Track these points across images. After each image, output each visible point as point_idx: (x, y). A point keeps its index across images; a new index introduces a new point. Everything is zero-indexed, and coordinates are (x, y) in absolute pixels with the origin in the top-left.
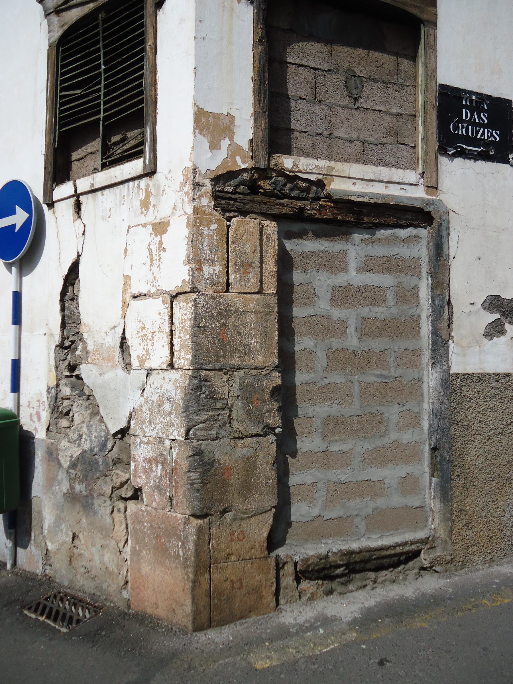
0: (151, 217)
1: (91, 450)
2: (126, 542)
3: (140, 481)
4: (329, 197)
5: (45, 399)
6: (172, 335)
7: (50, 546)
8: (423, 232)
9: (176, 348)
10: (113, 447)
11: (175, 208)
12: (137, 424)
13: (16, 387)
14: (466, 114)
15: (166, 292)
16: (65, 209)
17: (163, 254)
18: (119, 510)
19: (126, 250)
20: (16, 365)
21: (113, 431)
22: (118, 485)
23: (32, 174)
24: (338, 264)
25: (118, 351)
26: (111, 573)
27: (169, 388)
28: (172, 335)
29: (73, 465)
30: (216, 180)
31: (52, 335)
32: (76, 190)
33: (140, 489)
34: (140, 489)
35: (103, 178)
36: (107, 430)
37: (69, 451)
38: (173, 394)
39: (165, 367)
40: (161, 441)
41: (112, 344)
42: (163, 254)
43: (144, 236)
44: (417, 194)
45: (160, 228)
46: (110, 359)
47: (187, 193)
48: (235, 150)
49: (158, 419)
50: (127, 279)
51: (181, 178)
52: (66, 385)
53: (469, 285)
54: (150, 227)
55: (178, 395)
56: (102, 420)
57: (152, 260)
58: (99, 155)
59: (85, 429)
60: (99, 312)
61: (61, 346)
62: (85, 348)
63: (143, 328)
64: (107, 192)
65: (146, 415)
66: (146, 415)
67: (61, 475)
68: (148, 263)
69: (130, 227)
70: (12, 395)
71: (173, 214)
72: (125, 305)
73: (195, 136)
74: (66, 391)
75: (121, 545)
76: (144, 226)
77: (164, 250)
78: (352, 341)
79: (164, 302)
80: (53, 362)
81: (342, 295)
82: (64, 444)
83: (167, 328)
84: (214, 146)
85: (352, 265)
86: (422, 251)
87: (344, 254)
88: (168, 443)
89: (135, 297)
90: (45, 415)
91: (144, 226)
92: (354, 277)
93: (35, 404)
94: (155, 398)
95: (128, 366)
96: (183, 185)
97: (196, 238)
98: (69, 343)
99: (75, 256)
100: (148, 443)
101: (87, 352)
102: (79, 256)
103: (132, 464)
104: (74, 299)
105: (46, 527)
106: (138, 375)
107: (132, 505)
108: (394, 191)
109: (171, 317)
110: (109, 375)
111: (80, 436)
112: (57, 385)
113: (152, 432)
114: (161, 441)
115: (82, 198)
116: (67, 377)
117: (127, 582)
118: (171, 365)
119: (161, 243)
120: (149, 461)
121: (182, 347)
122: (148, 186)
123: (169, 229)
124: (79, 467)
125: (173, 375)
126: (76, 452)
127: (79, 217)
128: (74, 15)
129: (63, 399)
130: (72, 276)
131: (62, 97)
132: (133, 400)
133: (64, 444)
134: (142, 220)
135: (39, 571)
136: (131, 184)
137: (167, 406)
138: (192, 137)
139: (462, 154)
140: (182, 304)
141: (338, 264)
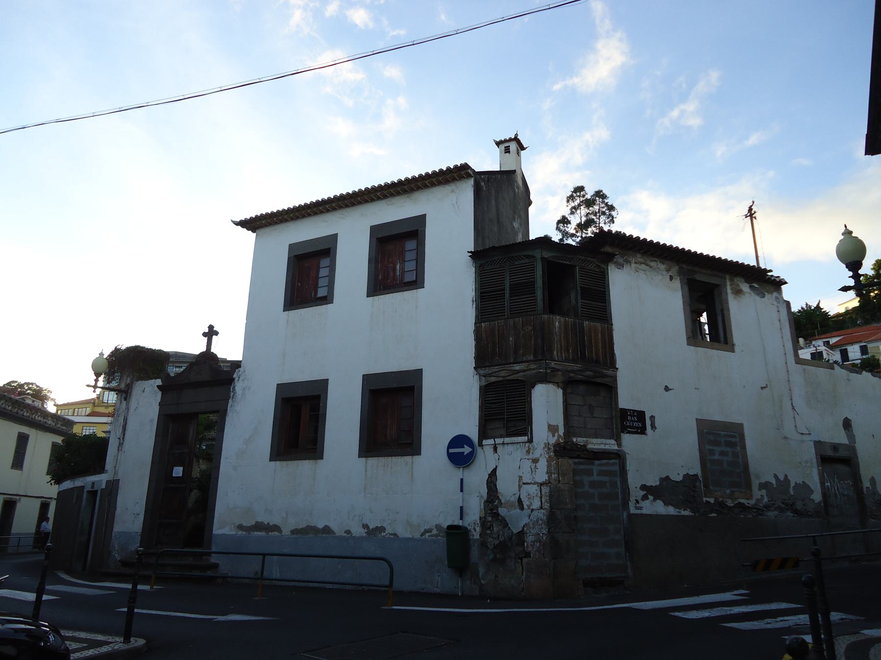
0: (531, 456)
4: (587, 450)
8: (617, 461)
13: (461, 518)
14: (629, 418)
16: (489, 450)
24: (590, 473)
27: (541, 515)
29: (495, 547)
30: (554, 446)
33: (529, 553)
34: (529, 553)
35: (507, 440)
37: (492, 542)
40: (539, 534)
43: (527, 464)
44: (616, 447)
45: (535, 461)
48: (559, 436)
50: (520, 477)
53: (634, 480)
60: (507, 488)
61: (486, 502)
66: (531, 526)
72: (520, 487)
81: (593, 484)
84: (554, 436)
85: (595, 473)
86: (616, 468)
90: (478, 529)
92: (595, 477)
95: (522, 508)
97: (549, 466)
106: (527, 511)
107: (525, 560)
108: (607, 447)
114: (539, 534)
120: (534, 542)
125: (542, 511)
126: (497, 542)
128: (493, 379)
132: (525, 520)
137: (540, 522)
139: (629, 432)
141: (590, 473)
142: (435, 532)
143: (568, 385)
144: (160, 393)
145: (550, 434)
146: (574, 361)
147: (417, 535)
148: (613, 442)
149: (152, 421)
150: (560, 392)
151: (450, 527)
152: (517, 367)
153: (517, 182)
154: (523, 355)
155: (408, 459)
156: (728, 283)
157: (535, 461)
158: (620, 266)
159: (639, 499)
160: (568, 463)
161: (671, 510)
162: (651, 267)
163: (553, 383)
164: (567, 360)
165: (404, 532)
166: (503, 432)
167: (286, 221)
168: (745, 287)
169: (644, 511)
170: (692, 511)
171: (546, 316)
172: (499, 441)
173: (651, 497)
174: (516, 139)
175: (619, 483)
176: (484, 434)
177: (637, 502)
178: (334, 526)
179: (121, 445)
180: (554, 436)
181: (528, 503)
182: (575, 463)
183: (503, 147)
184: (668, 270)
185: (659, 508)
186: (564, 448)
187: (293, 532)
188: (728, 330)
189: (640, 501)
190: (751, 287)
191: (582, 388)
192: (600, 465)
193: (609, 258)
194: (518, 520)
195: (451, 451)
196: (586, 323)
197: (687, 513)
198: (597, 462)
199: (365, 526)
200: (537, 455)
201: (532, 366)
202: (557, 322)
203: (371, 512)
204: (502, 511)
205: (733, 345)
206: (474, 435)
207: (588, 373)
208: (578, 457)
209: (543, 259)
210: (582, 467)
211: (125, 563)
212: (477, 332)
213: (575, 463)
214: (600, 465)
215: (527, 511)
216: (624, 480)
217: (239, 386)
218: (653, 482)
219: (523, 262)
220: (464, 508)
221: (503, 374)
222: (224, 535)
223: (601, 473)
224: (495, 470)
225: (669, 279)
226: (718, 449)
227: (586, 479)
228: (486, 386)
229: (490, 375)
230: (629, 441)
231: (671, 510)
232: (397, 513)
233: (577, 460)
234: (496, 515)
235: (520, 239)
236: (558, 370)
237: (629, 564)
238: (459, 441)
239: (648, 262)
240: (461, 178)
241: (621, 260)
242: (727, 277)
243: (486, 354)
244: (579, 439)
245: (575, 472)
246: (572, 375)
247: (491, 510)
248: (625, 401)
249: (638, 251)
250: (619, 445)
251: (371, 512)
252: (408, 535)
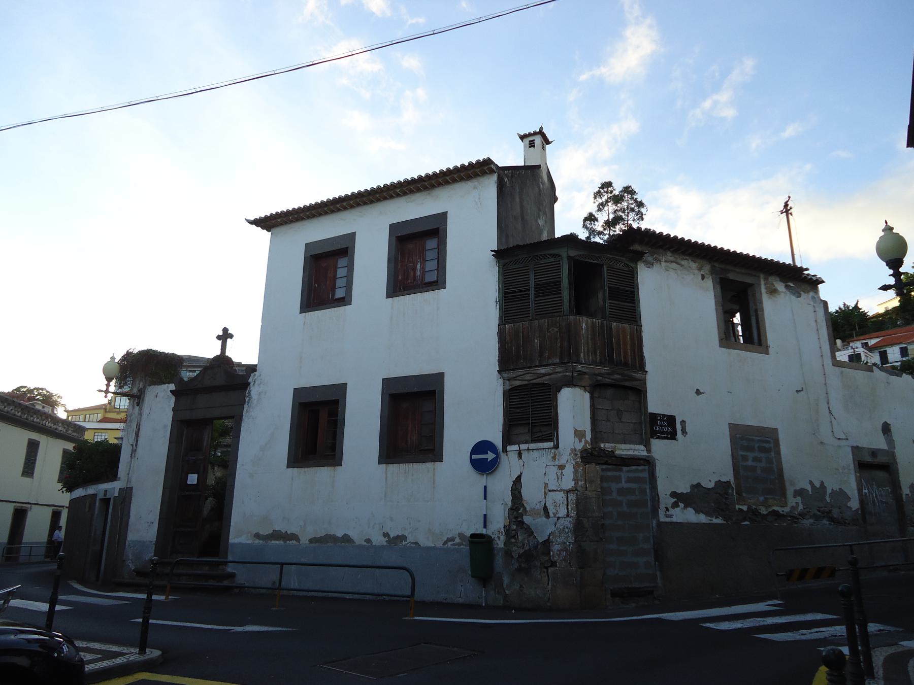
0: (557, 463)
1: (530, 549)
4: (615, 456)
7: (507, 592)
8: (647, 467)
13: (485, 526)
16: (513, 456)
24: (618, 480)
27: (567, 523)
29: (520, 556)
30: (581, 452)
33: (555, 562)
34: (555, 562)
35: (532, 446)
37: (517, 551)
40: (565, 543)
43: (553, 471)
44: (645, 453)
45: (561, 467)
46: (539, 514)
48: (586, 442)
50: (546, 485)
53: (664, 487)
60: (532, 495)
61: (511, 509)
62: (525, 509)
72: (545, 494)
78: (625, 509)
81: (621, 491)
84: (580, 441)
85: (623, 480)
87: (620, 476)
90: (502, 538)
92: (624, 485)
95: (548, 516)
97: (575, 473)
106: (553, 520)
107: (551, 570)
108: (636, 453)
110: (539, 520)
114: (565, 543)
125: (569, 519)
126: (522, 551)
128: (517, 383)
132: (551, 529)
133: (514, 548)
139: (659, 438)
141: (618, 480)
142: (457, 540)
143: (596, 389)
144: (173, 399)
145: (577, 440)
146: (602, 364)
147: (439, 544)
148: (642, 447)
149: (165, 427)
150: (587, 395)
151: (473, 536)
152: (542, 370)
153: (542, 178)
154: (549, 358)
155: (429, 465)
156: (762, 282)
157: (561, 467)
158: (650, 265)
159: (669, 506)
160: (595, 469)
161: (702, 518)
162: (682, 266)
163: (580, 386)
164: (594, 363)
165: (425, 542)
166: (528, 438)
167: (303, 219)
168: (780, 286)
169: (674, 519)
170: (725, 518)
171: (572, 317)
172: (524, 446)
173: (682, 505)
174: (541, 133)
175: (648, 491)
176: (508, 439)
177: (667, 509)
178: (353, 534)
179: (134, 451)
180: (580, 441)
181: (554, 511)
182: (603, 470)
183: (527, 141)
184: (700, 269)
185: (689, 516)
186: (592, 454)
187: (311, 541)
188: (762, 332)
189: (671, 509)
190: (787, 287)
191: (609, 392)
192: (628, 471)
193: (638, 257)
194: (544, 529)
195: (474, 457)
196: (614, 325)
197: (719, 521)
198: (625, 469)
199: (386, 535)
200: (563, 461)
201: (558, 370)
202: (585, 323)
203: (392, 519)
204: (527, 519)
205: (767, 347)
206: (498, 441)
207: (616, 376)
208: (606, 463)
209: (569, 258)
210: (610, 474)
211: (139, 573)
212: (501, 334)
213: (603, 470)
214: (628, 471)
215: (553, 520)
216: (654, 487)
217: (254, 391)
218: (684, 488)
219: (548, 260)
221: (528, 377)
222: (240, 544)
223: (629, 480)
224: (519, 477)
225: (700, 277)
226: (750, 455)
227: (614, 486)
228: (510, 390)
229: (514, 379)
230: (659, 447)
231: (702, 518)
232: (419, 521)
233: (604, 467)
234: (521, 524)
235: (545, 237)
236: (585, 373)
237: (658, 573)
238: (482, 447)
239: (679, 261)
240: (484, 173)
241: (650, 259)
242: (762, 276)
243: (508, 360)
244: (607, 445)
245: (603, 479)
246: (600, 378)
247: (516, 518)
248: (655, 405)
249: (669, 249)
250: (649, 451)
251: (392, 519)
252: (430, 544)
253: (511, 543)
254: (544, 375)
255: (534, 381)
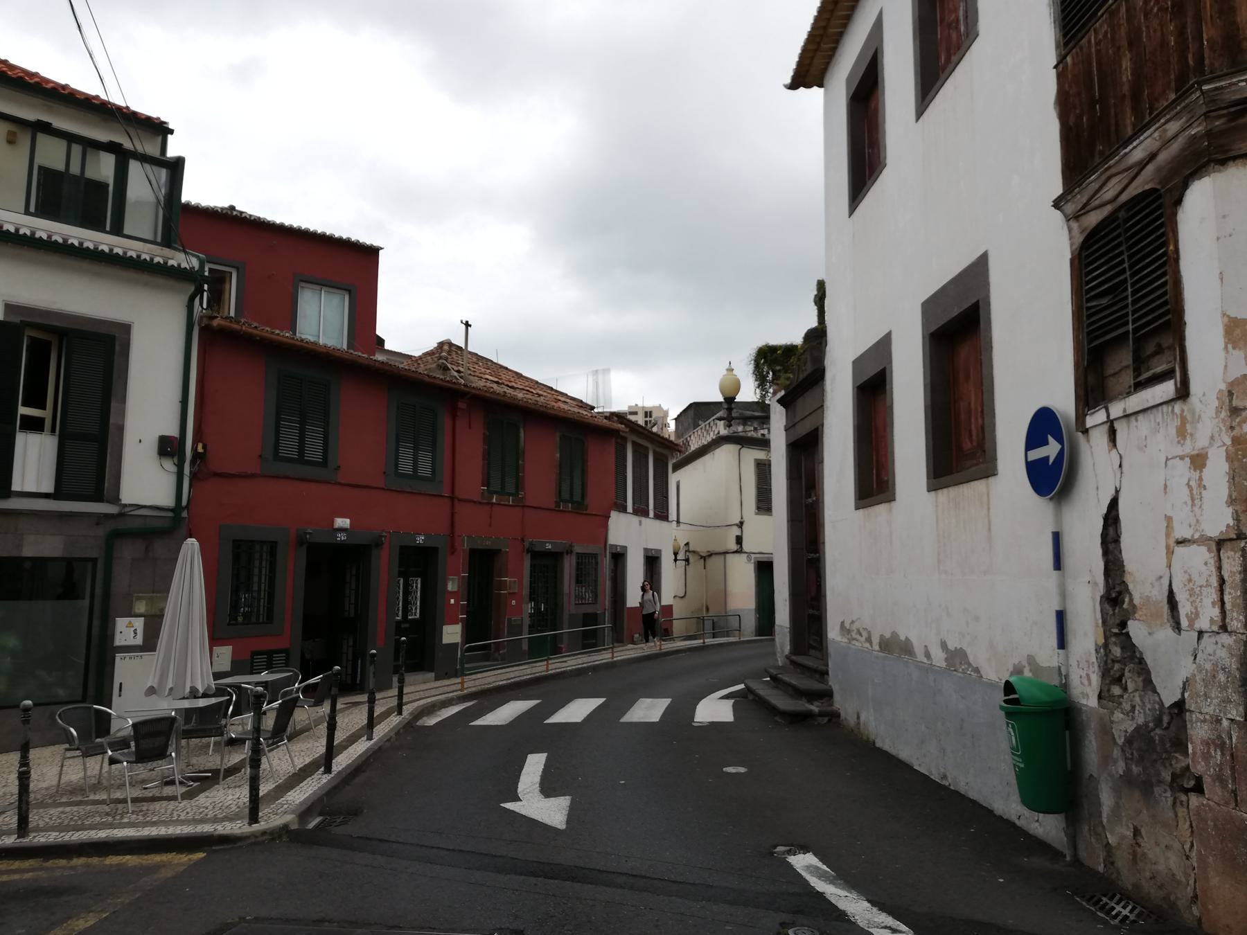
0: (1188, 448)
2: (1192, 845)
3: (1199, 768)
5: (1094, 660)
6: (1222, 591)
7: (1112, 840)
9: (1228, 606)
10: (1169, 723)
11: (1212, 438)
12: (1191, 697)
13: (1062, 643)
15: (1210, 539)
16: (1099, 438)
17: (1204, 492)
18: (1181, 803)
19: (1166, 486)
20: (1061, 616)
21: (1167, 705)
22: (1178, 771)
23: (1064, 401)
25: (1166, 608)
26: (1179, 883)
28: (1222, 591)
29: (1129, 741)
31: (1096, 584)
32: (1108, 416)
35: (1136, 401)
36: (1161, 703)
37: (1123, 725)
38: (1227, 662)
39: (1215, 628)
41: (1159, 598)
42: (1204, 492)
43: (1182, 470)
45: (1198, 461)
47: (1223, 420)
49: (1214, 693)
50: (1169, 520)
51: (1216, 403)
52: (1115, 644)
54: (1187, 460)
55: (1234, 665)
56: (1155, 691)
57: (1193, 500)
58: (1130, 372)
59: (1137, 699)
62: (1131, 600)
63: (1190, 580)
64: (1140, 417)
65: (1200, 688)
66: (1200, 688)
67: (1116, 753)
68: (1190, 503)
69: (1167, 459)
70: (1061, 651)
71: (1211, 445)
72: (1170, 552)
73: (1227, 352)
74: (1117, 651)
75: (1187, 847)
76: (1182, 458)
77: (1205, 488)
79: (1209, 551)
80: (1099, 615)
82: (1118, 716)
83: (1214, 581)
88: (1225, 723)
89: (1179, 543)
90: (1095, 679)
91: (1182, 458)
93: (1084, 665)
94: (1208, 666)
95: (1177, 627)
96: (1218, 410)
98: (1115, 595)
99: (1113, 492)
100: (1205, 721)
101: (1134, 606)
102: (1117, 491)
103: (1190, 746)
104: (1117, 540)
105: (1104, 815)
107: (1194, 800)
109: (1219, 568)
111: (1133, 707)
112: (1106, 645)
113: (1210, 709)
114: (1218, 721)
115: (1116, 425)
116: (1116, 634)
117: (1196, 896)
118: (1224, 628)
119: (1200, 479)
121: (1233, 606)
122: (1183, 411)
123: (1209, 463)
124: (1136, 745)
125: (1225, 639)
126: (1130, 727)
127: (1115, 445)
128: (1093, 219)
129: (1114, 661)
130: (1112, 518)
131: (1088, 308)
132: (1186, 668)
134: (1179, 451)
135: (1101, 868)
136: (1165, 407)
137: (1222, 677)
138: (1223, 354)
140: (1231, 553)
152: (1137, 152)
155: (979, 486)
172: (1116, 409)
200: (1202, 440)
201: (1173, 127)
204: (1136, 630)
220: (1070, 618)
221: (1109, 192)
224: (1114, 504)
229: (1085, 209)
253: (1112, 698)
254: (1142, 165)
255: (1124, 197)
